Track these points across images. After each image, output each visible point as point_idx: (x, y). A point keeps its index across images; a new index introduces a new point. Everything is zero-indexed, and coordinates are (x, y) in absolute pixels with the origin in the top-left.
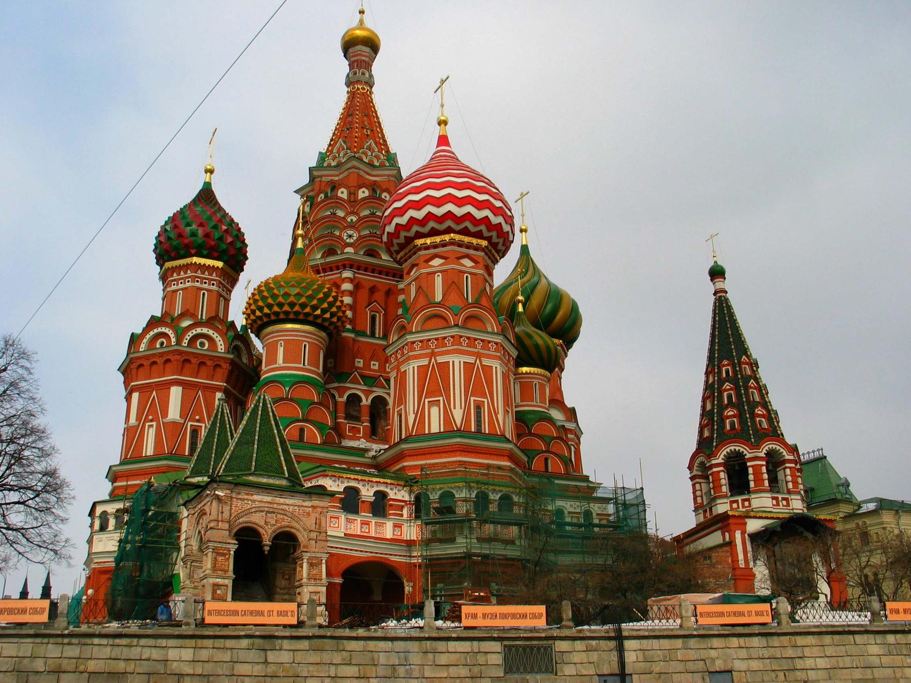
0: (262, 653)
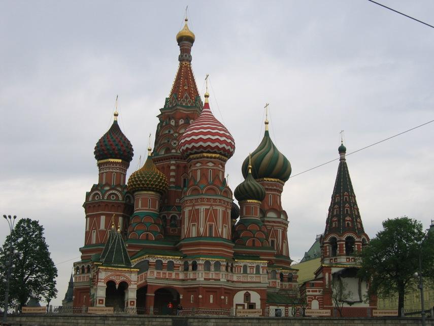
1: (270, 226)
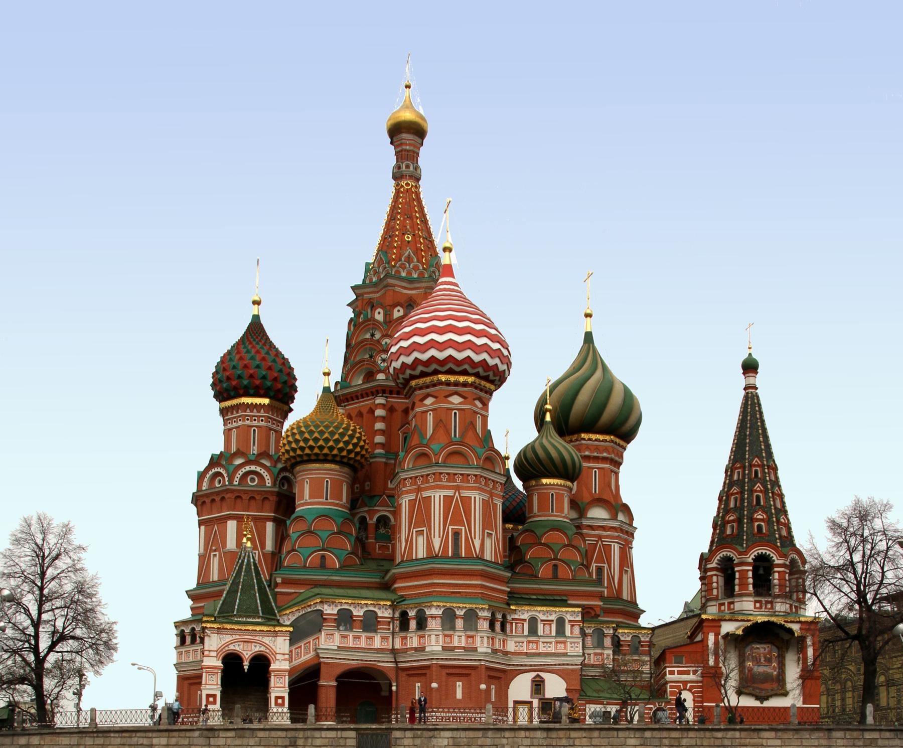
0: (207, 739)
1: (593, 536)
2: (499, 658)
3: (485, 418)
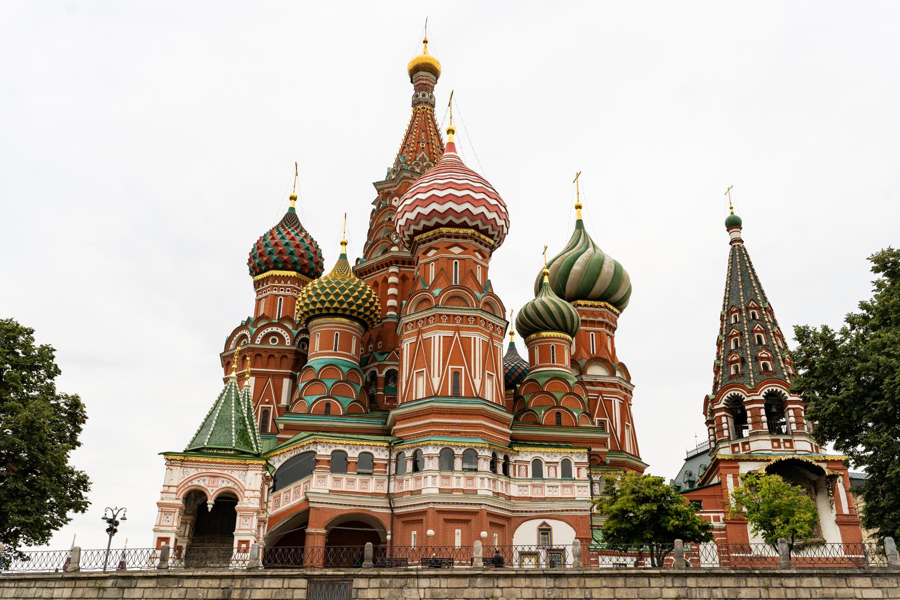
2: (501, 503)
3: (485, 269)
